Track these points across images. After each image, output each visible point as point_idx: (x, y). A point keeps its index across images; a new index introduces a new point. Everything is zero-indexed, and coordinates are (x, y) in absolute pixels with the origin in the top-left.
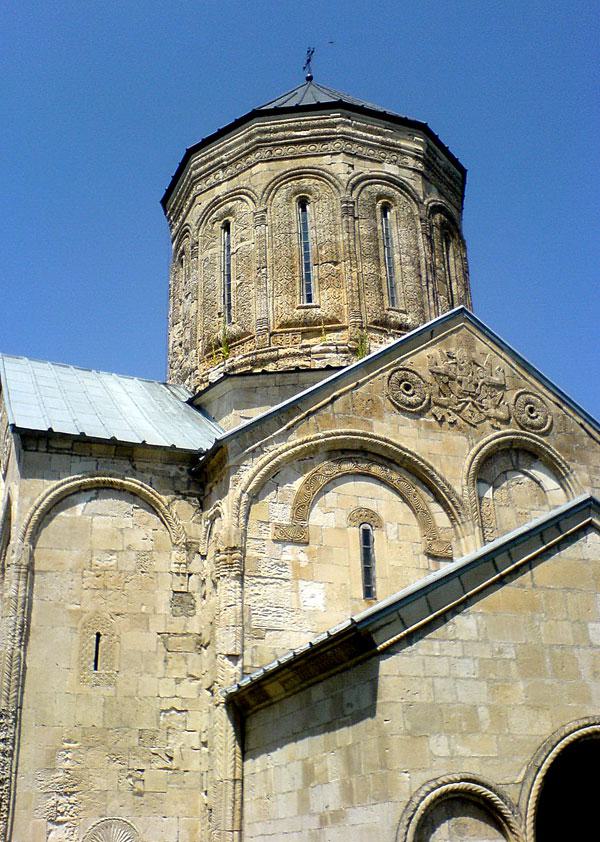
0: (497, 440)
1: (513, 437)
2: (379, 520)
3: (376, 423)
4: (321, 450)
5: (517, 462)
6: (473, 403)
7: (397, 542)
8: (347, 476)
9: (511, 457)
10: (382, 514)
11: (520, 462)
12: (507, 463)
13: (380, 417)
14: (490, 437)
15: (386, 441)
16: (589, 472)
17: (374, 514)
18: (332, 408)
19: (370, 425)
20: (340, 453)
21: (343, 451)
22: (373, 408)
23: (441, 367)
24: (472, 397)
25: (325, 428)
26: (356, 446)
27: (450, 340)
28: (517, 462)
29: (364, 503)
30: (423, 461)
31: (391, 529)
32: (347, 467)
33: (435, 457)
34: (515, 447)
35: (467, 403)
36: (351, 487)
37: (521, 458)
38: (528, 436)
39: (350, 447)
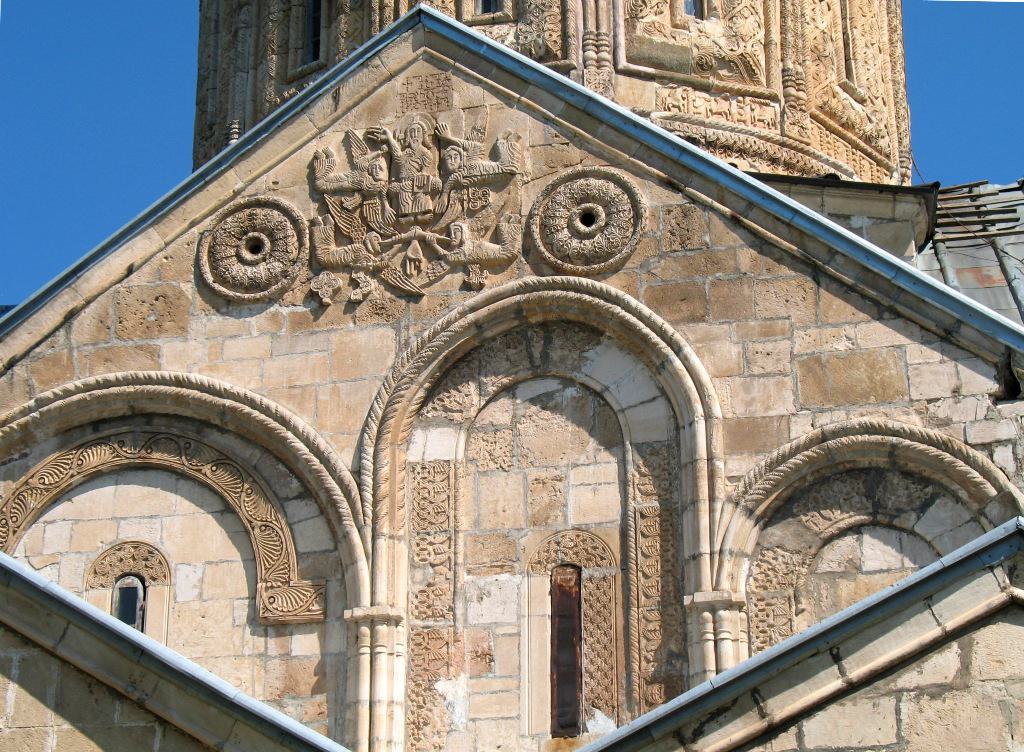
0: (471, 317)
1: (518, 298)
2: (163, 562)
3: (167, 346)
4: (39, 434)
5: (545, 356)
6: (423, 241)
7: (196, 605)
8: (95, 478)
9: (529, 347)
10: (169, 548)
11: (555, 355)
12: (514, 364)
13: (182, 331)
14: (451, 307)
15: (179, 382)
16: (743, 341)
17: (152, 551)
18: (68, 338)
19: (154, 354)
20: (89, 430)
21: (96, 425)
22: (166, 312)
23: (338, 172)
24: (424, 225)
25: (59, 379)
26: (121, 409)
27: (383, 100)
28: (545, 356)
29: (131, 532)
30: (266, 410)
31: (185, 579)
32: (98, 457)
33: (296, 392)
34: (533, 320)
35: (407, 243)
36: (104, 497)
37: (557, 342)
38: (578, 288)
39: (106, 415)
